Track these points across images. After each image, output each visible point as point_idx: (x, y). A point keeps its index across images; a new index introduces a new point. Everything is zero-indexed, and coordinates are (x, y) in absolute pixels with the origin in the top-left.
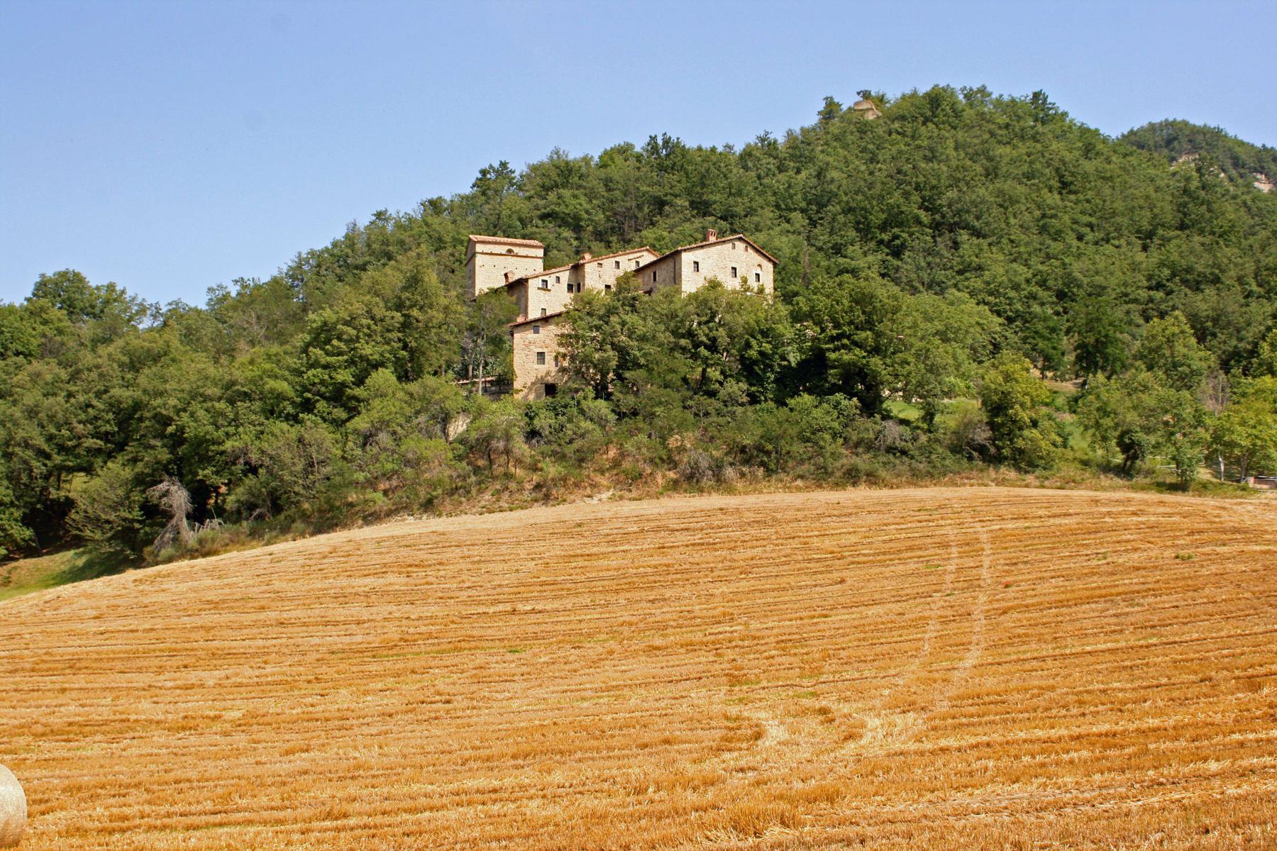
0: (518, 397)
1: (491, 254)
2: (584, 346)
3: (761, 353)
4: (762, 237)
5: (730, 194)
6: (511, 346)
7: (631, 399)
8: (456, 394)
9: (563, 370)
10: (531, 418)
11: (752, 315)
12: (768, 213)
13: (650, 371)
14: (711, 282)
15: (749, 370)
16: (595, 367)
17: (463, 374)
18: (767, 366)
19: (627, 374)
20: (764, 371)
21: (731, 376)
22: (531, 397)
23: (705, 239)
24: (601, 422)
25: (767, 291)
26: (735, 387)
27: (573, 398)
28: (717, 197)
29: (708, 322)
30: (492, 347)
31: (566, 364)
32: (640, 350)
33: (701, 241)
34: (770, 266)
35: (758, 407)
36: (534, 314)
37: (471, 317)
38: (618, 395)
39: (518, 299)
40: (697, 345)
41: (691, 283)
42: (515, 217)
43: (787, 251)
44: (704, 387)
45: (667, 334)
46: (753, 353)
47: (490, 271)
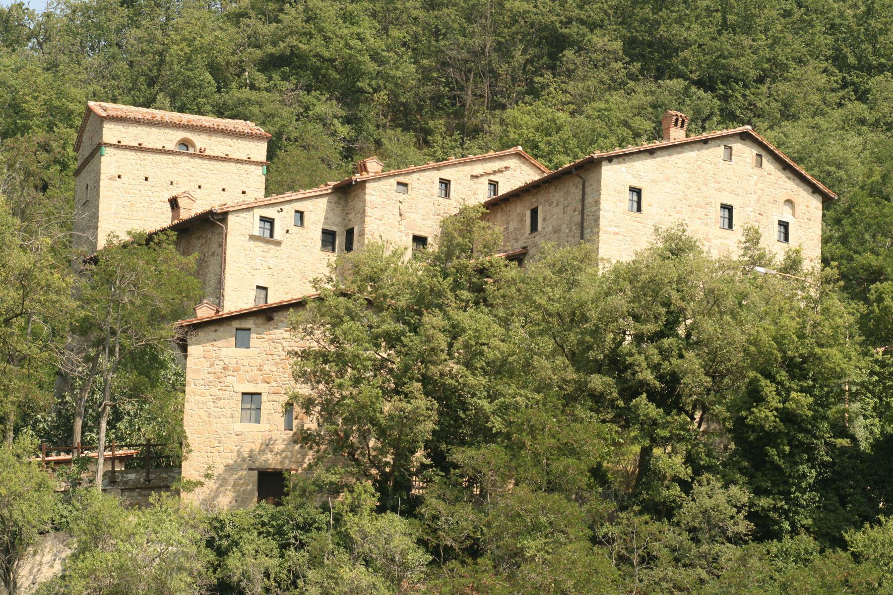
0: (192, 500)
1: (140, 149)
2: (357, 381)
3: (788, 417)
4: (796, 134)
5: (725, 25)
6: (181, 375)
7: (465, 517)
8: (40, 487)
9: (305, 438)
10: (221, 553)
11: (766, 323)
12: (816, 76)
13: (514, 448)
14: (669, 238)
15: (756, 455)
16: (382, 433)
17: (58, 437)
18: (798, 447)
19: (459, 455)
20: (791, 459)
21: (709, 468)
22: (225, 501)
23: (659, 133)
24: (392, 570)
25: (806, 266)
26: (721, 497)
27: (325, 508)
28: (693, 32)
29: (660, 335)
30: (133, 376)
31: (311, 424)
32: (492, 398)
33: (649, 139)
34: (816, 203)
35: (774, 546)
36: (238, 297)
37: (86, 302)
38: (433, 504)
39: (202, 263)
40: (630, 391)
41: (621, 239)
42: (200, 60)
43: (858, 169)
44: (644, 494)
45: (560, 360)
46: (766, 415)
47: (142, 179)
